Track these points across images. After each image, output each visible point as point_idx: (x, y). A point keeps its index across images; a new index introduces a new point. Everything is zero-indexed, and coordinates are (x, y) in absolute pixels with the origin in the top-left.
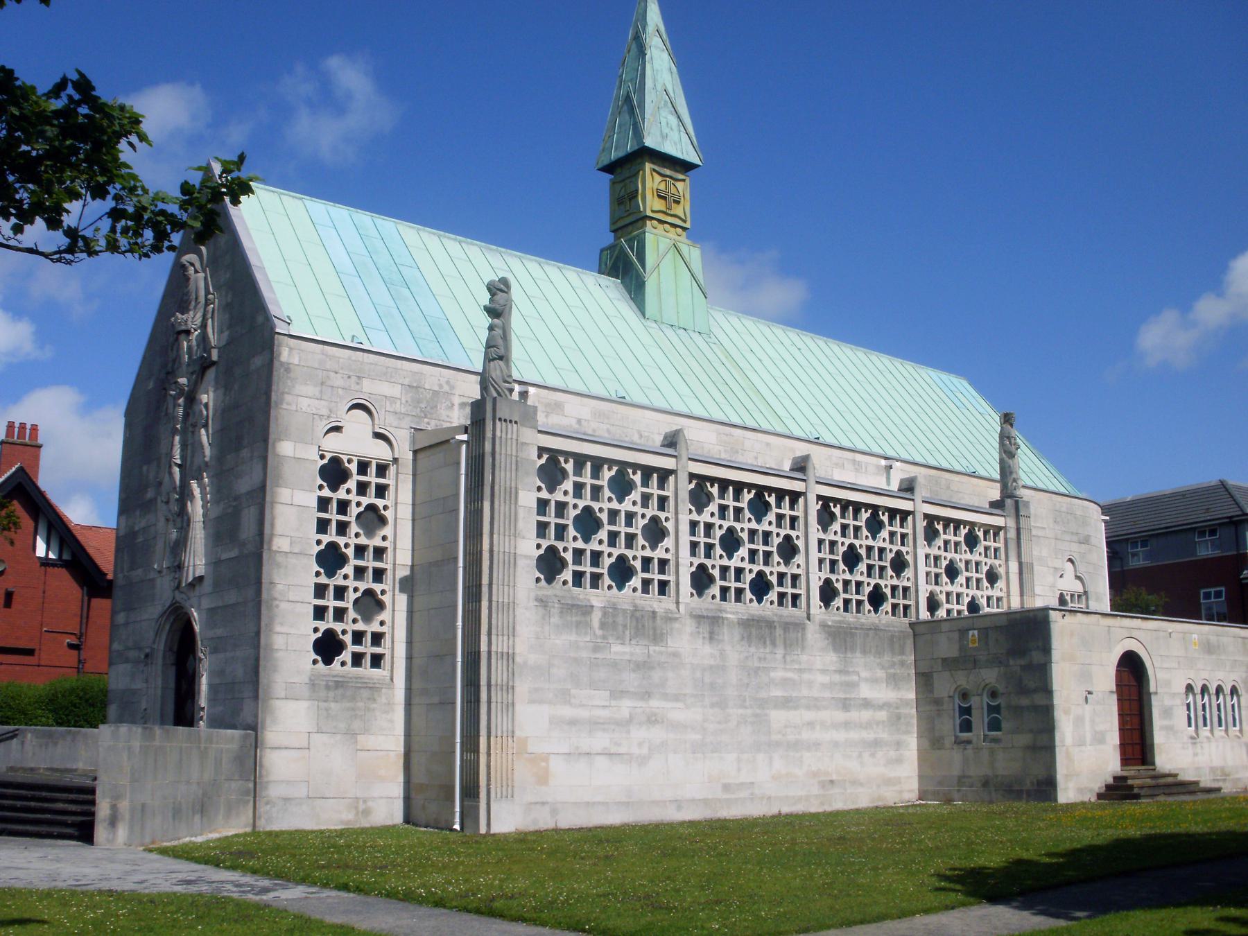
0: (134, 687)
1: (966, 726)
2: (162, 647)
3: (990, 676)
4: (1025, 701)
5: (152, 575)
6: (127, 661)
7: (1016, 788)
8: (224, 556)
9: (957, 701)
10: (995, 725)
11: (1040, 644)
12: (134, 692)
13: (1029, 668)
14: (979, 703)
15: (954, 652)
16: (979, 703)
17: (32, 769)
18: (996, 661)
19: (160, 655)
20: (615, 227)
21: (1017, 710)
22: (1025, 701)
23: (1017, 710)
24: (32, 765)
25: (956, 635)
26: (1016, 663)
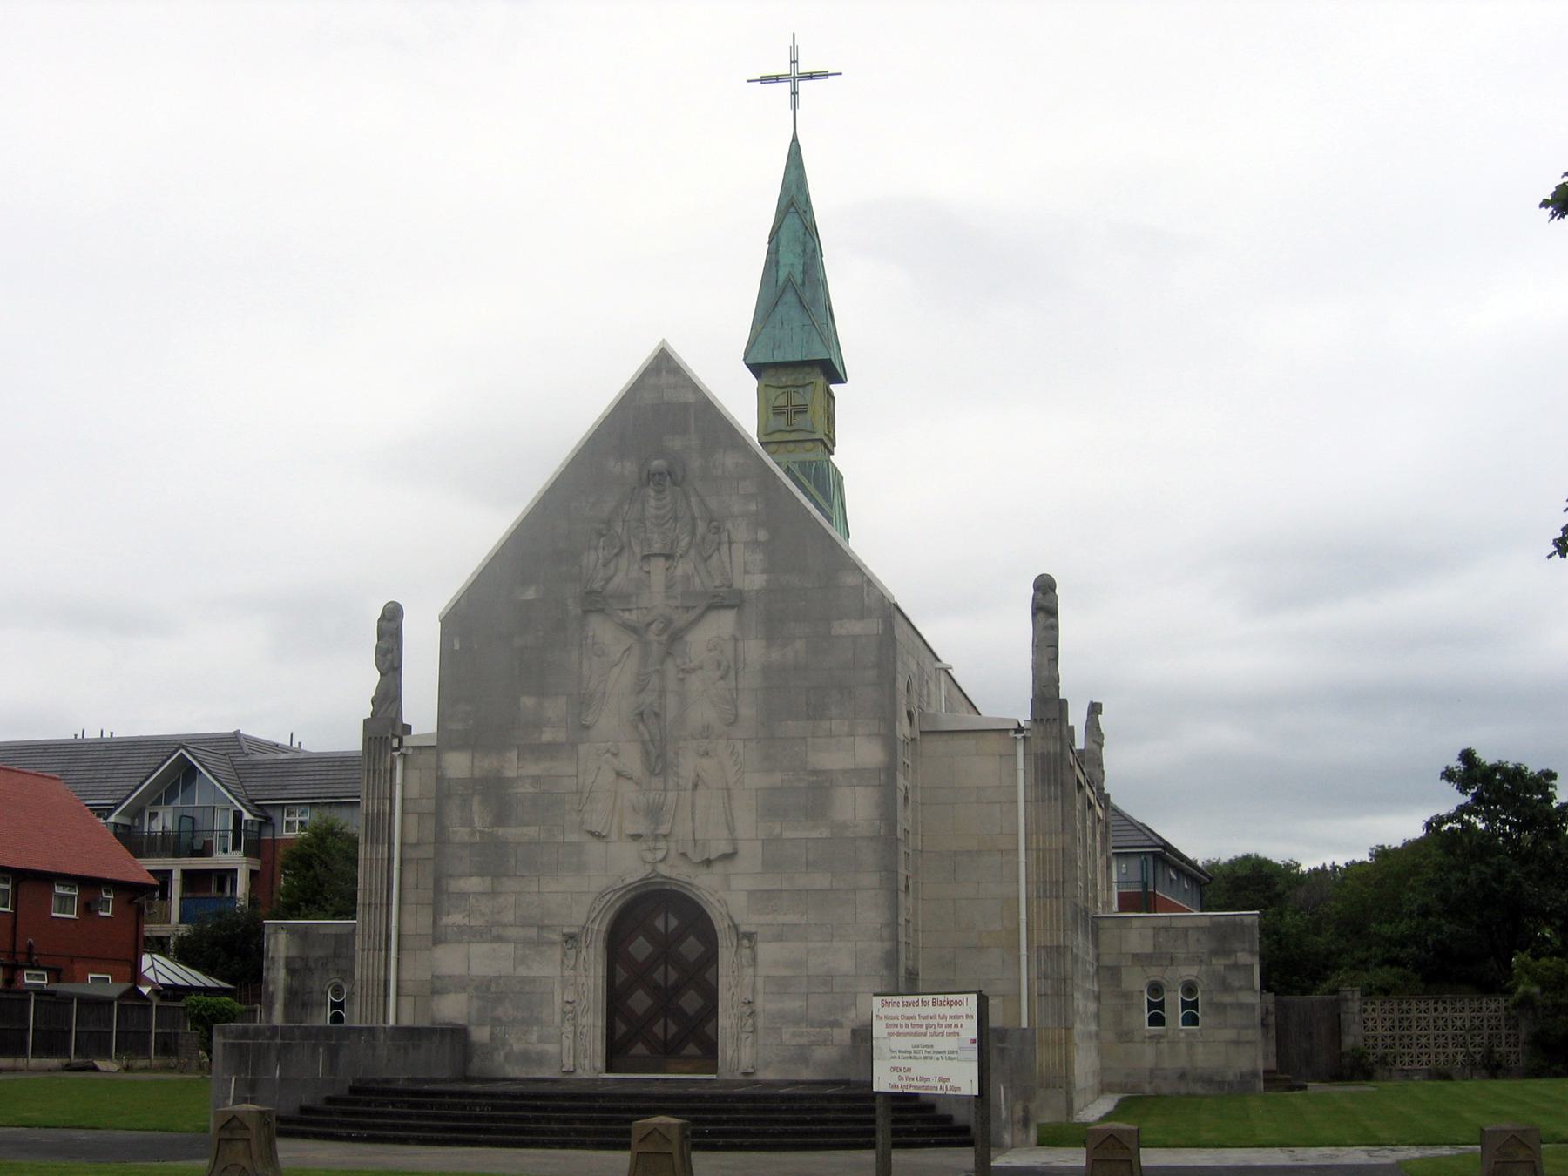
0: (522, 971)
1: (1157, 1020)
2: (604, 928)
3: (1189, 972)
4: (1228, 999)
5: (573, 837)
6: (499, 939)
7: (1217, 1078)
8: (787, 834)
9: (1146, 996)
10: (1191, 1020)
11: (1247, 946)
12: (533, 980)
13: (1235, 967)
14: (1174, 1000)
15: (1148, 948)
16: (1174, 1000)
17: (387, 1081)
18: (1196, 959)
19: (601, 936)
20: (764, 439)
21: (1220, 1008)
22: (1228, 999)
23: (1220, 1008)
24: (386, 1075)
25: (1150, 932)
26: (1219, 963)
